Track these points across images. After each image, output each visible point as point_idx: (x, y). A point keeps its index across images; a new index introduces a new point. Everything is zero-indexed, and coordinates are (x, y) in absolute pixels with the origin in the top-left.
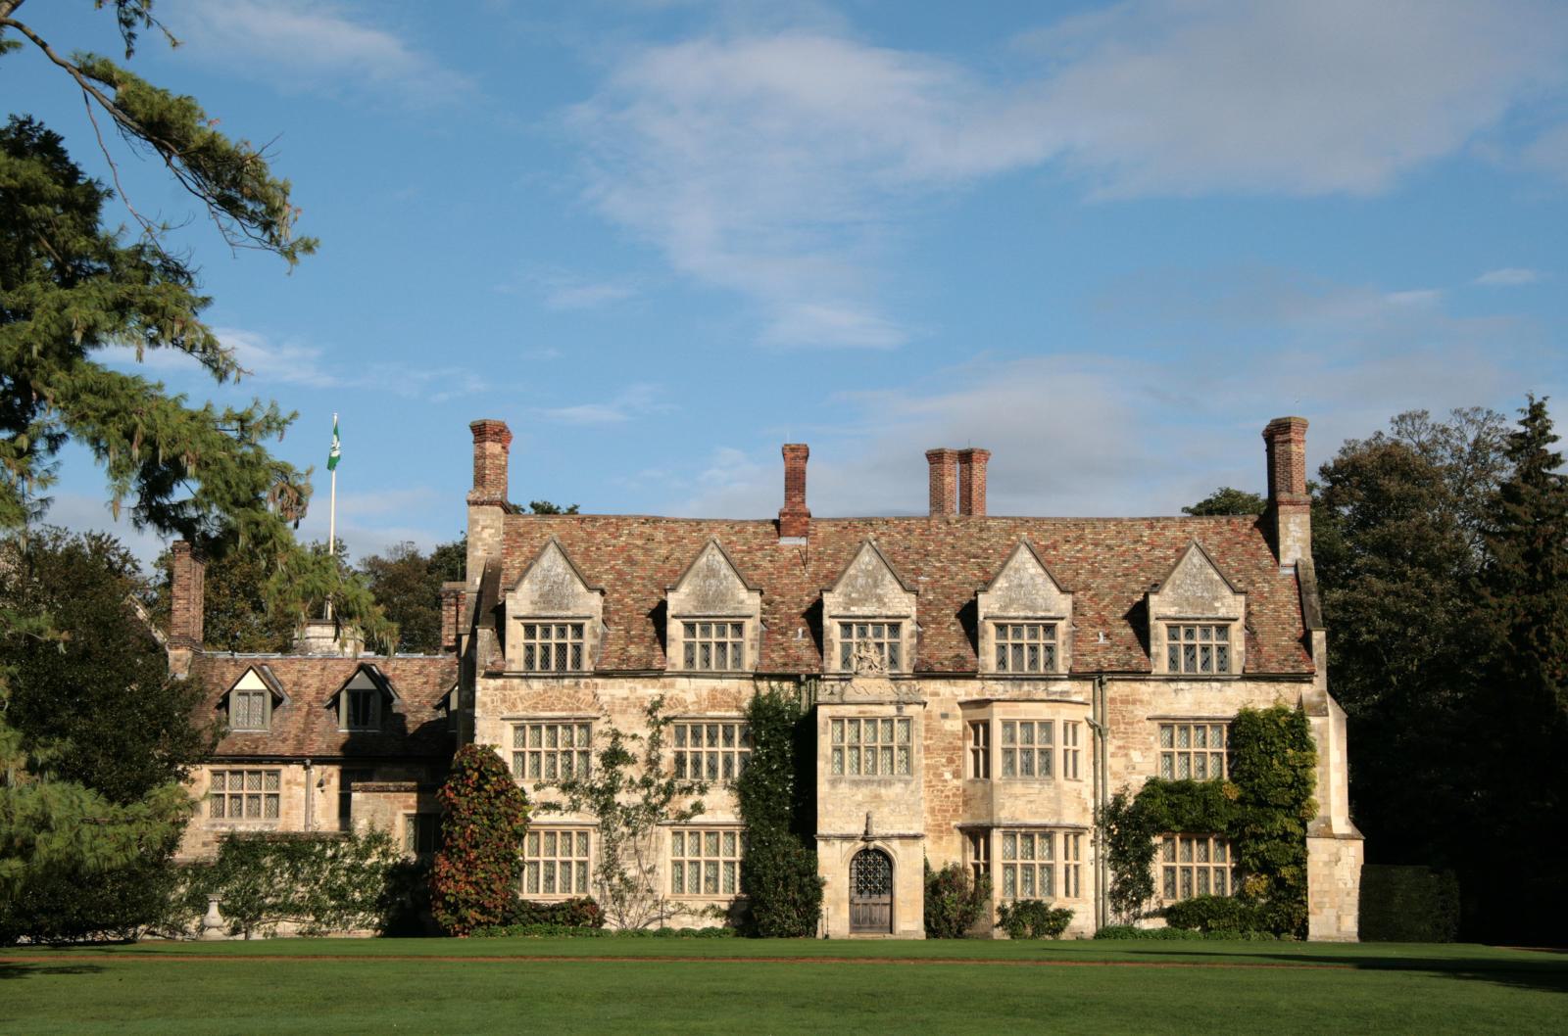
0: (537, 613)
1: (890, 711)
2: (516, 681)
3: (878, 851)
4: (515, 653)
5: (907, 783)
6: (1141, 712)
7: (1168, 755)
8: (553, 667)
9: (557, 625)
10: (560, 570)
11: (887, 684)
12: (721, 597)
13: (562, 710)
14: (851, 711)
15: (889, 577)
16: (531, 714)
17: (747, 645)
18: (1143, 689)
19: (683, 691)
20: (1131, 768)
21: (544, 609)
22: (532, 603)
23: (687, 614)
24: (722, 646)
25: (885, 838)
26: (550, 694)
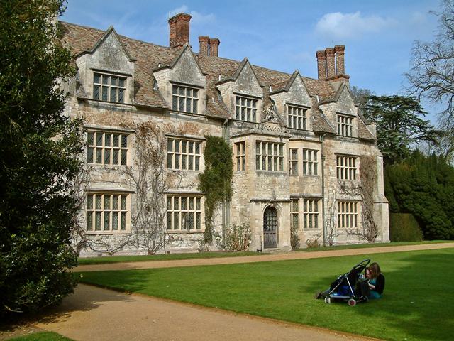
0: (102, 68)
1: (278, 140)
4: (88, 89)
6: (333, 151)
7: (338, 168)
9: (112, 77)
10: (114, 46)
12: (190, 75)
13: (116, 125)
16: (99, 126)
17: (199, 103)
18: (333, 142)
19: (173, 121)
20: (329, 173)
21: (106, 67)
22: (100, 62)
23: (175, 81)
24: (189, 100)
25: (279, 202)
26: (109, 115)
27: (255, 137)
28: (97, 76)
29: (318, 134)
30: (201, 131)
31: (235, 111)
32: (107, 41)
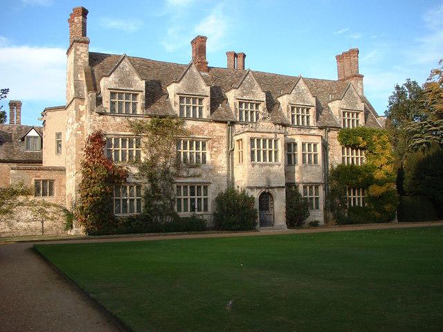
1: (272, 136)
2: (109, 117)
3: (269, 193)
4: (106, 104)
5: (279, 165)
7: (343, 158)
8: (124, 112)
10: (127, 69)
11: (271, 124)
14: (259, 135)
15: (257, 85)
27: (250, 135)
28: (113, 95)
29: (321, 128)
30: (206, 132)
31: (238, 114)
32: (121, 66)
